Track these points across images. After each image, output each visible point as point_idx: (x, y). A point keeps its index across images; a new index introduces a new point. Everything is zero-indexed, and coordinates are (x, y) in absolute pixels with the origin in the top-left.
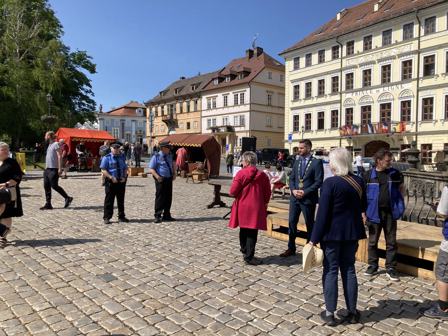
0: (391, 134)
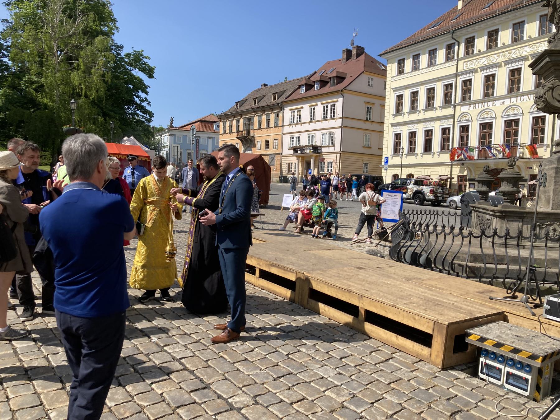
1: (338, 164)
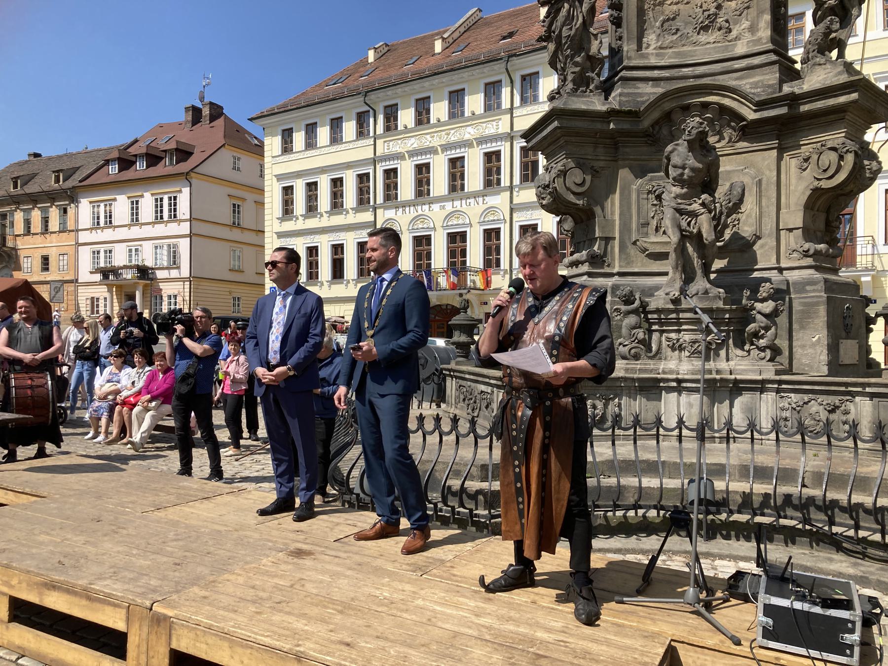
0: (465, 291)
1: (188, 298)
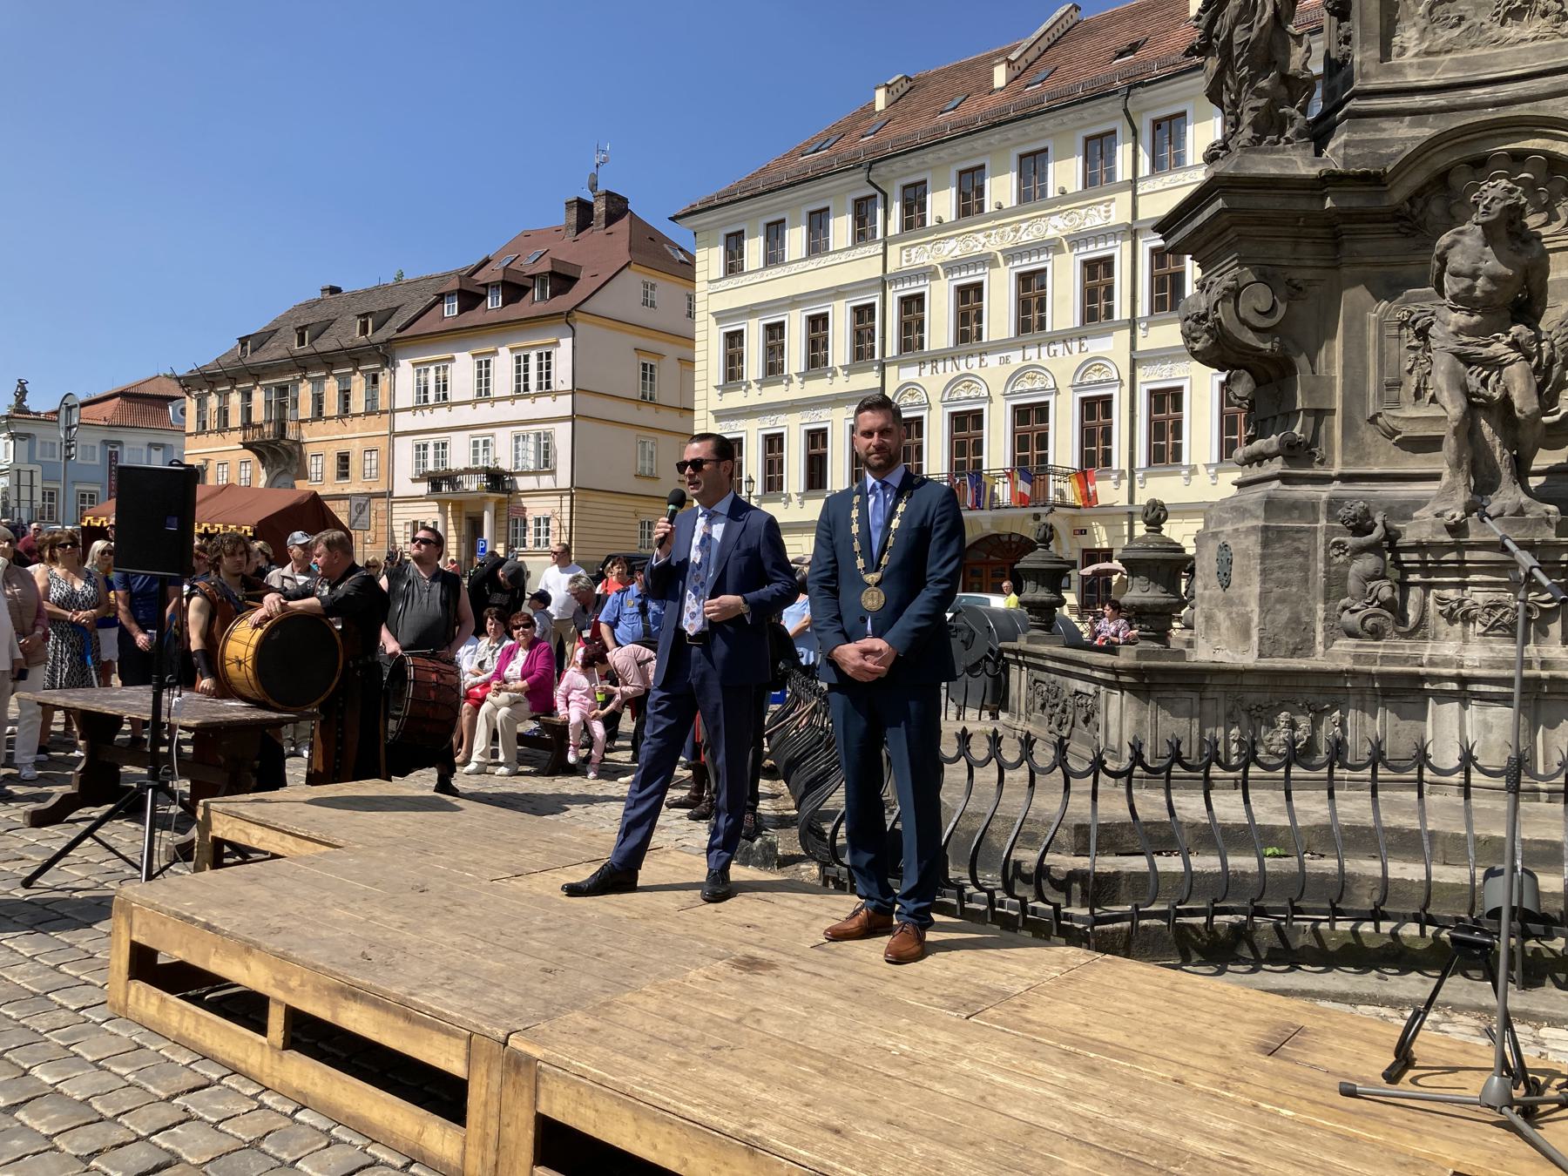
0: (1046, 510)
1: (567, 523)
